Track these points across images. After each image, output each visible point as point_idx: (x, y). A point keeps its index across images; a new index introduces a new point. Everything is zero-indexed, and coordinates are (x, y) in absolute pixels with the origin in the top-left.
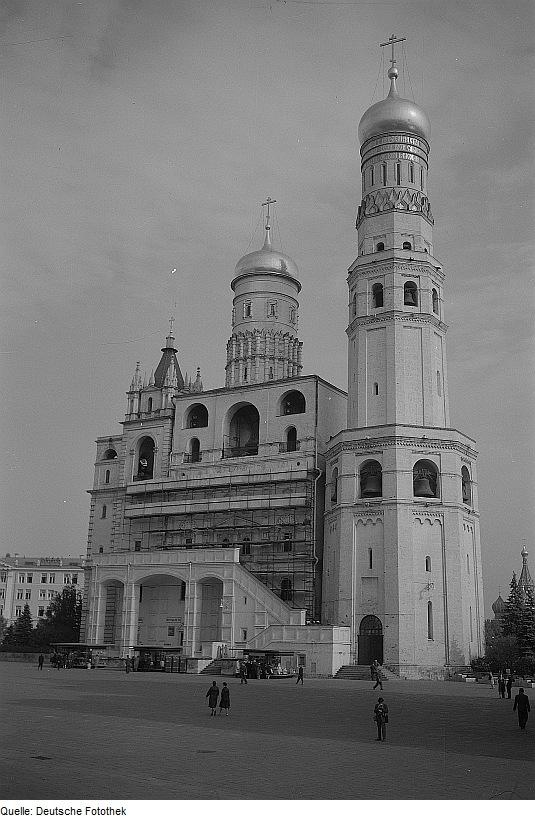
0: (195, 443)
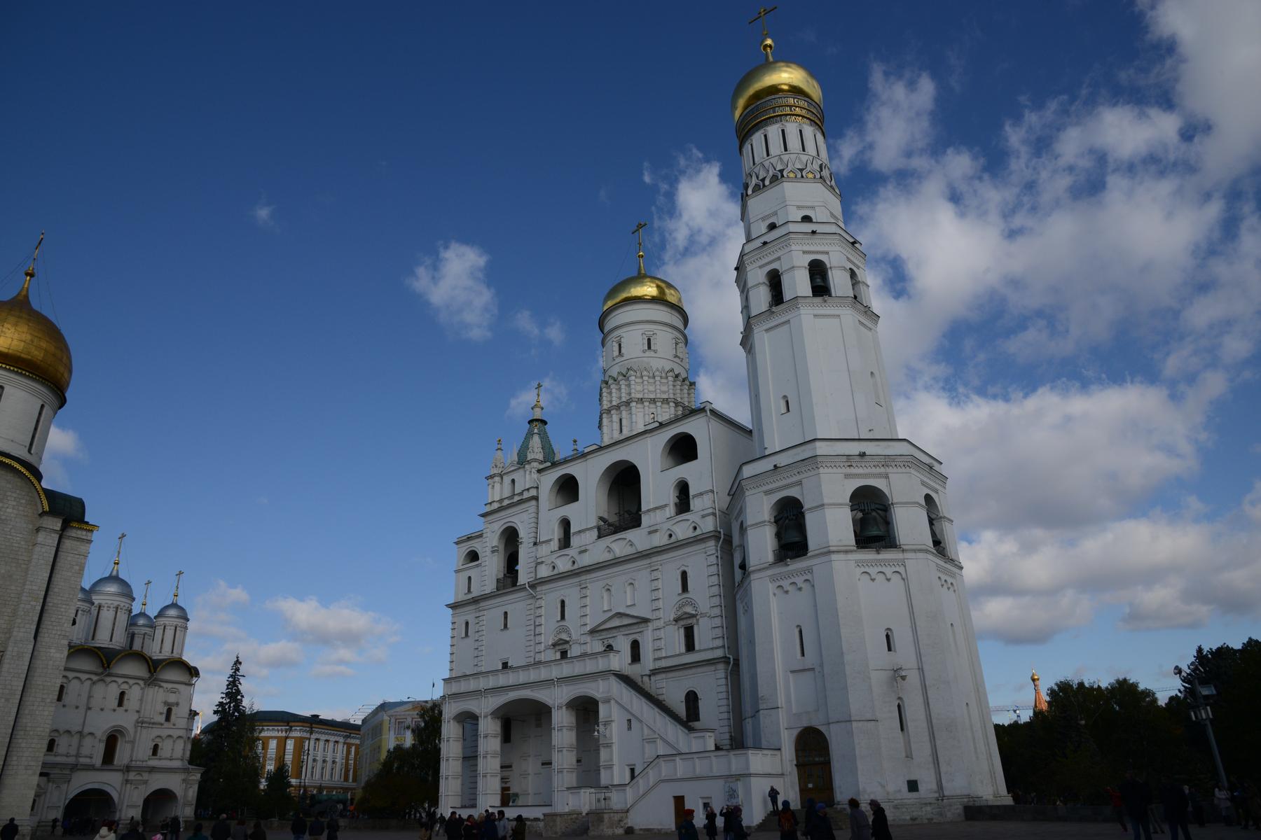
0: (566, 524)
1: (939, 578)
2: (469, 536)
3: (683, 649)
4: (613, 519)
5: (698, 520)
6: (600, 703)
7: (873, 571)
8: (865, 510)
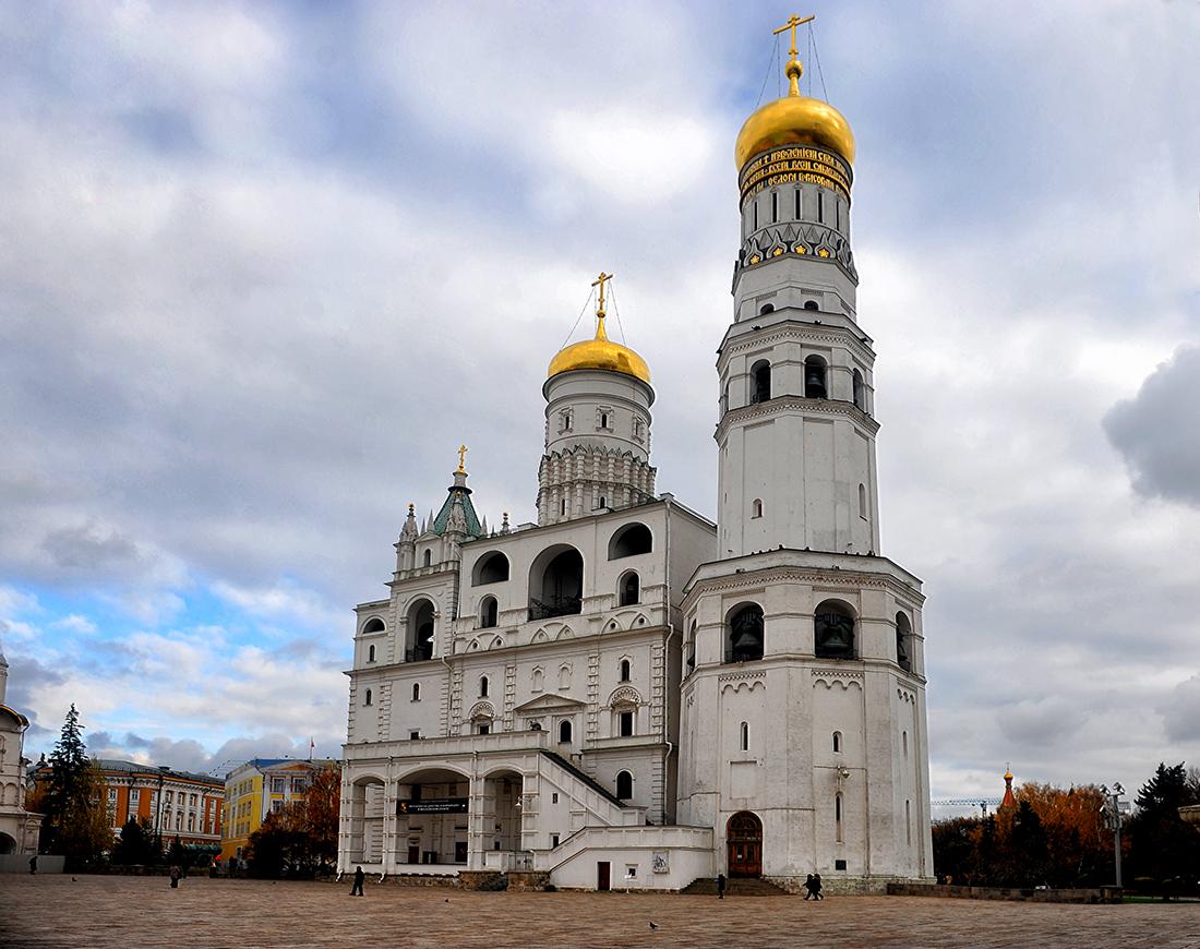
4: (550, 603)
5: (645, 612)
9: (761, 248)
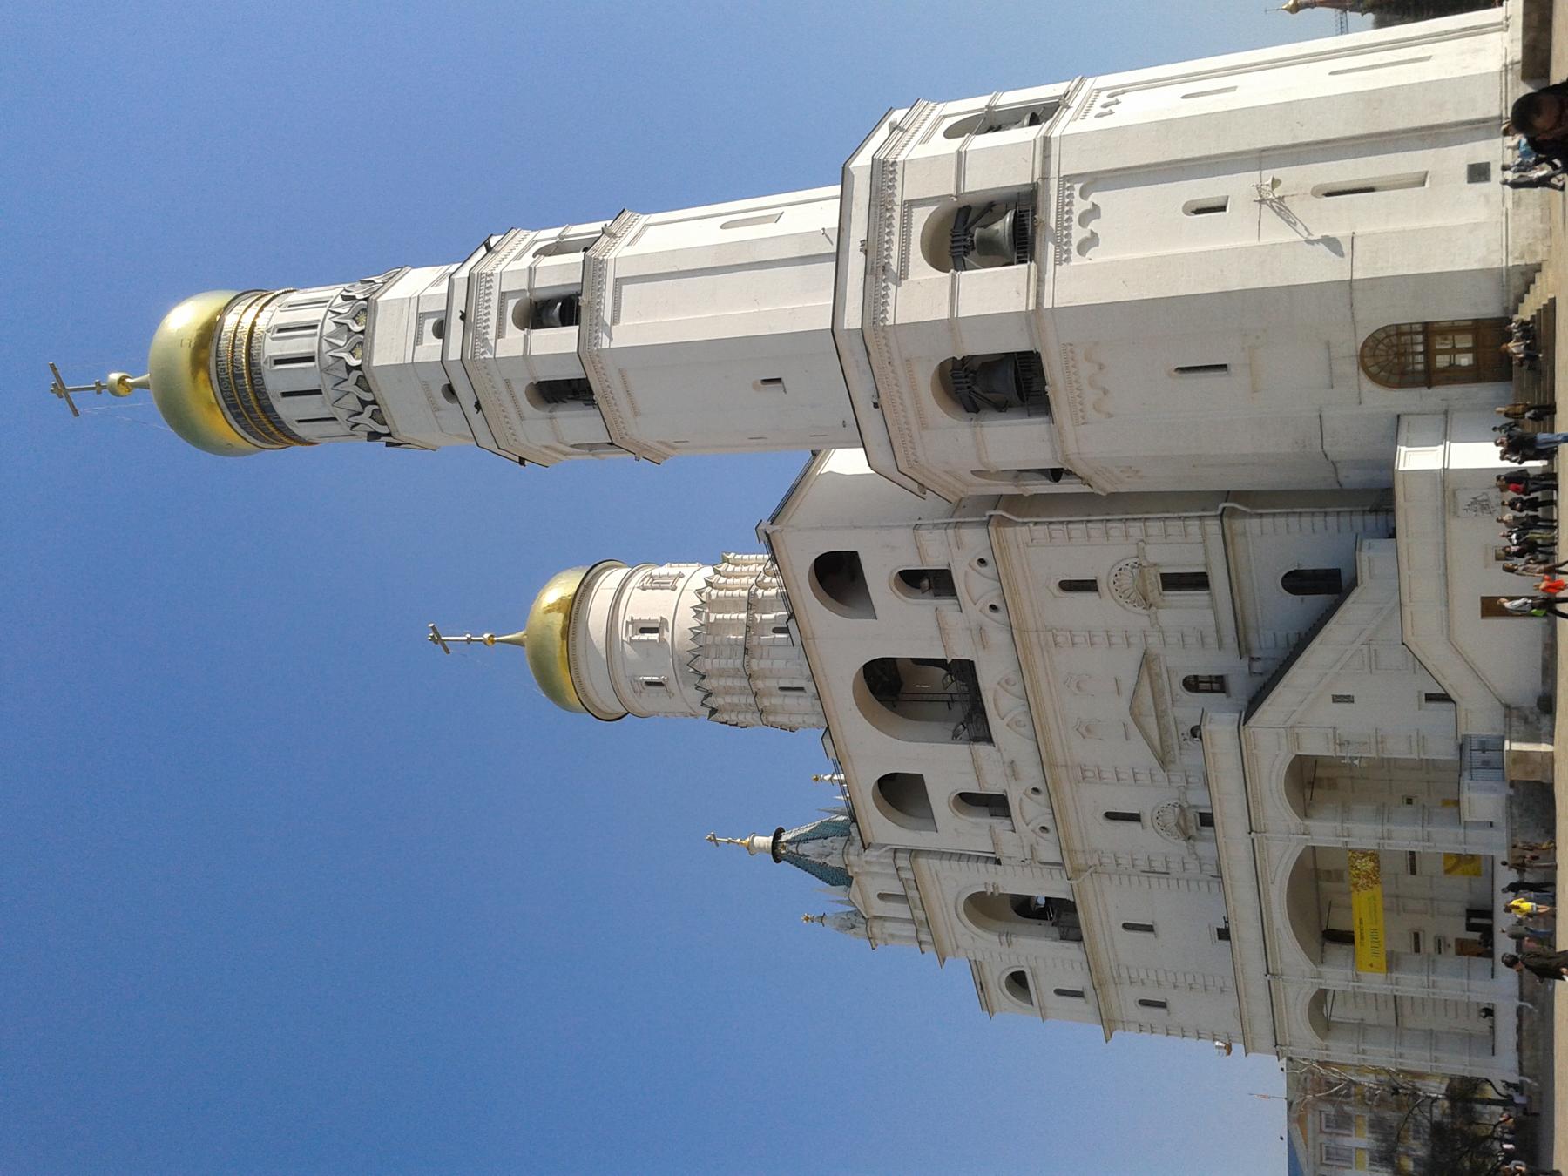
0: (969, 801)
1: (1097, 116)
2: (979, 987)
3: (1199, 597)
4: (959, 710)
6: (1299, 753)
7: (1078, 234)
8: (965, 247)
9: (359, 408)
